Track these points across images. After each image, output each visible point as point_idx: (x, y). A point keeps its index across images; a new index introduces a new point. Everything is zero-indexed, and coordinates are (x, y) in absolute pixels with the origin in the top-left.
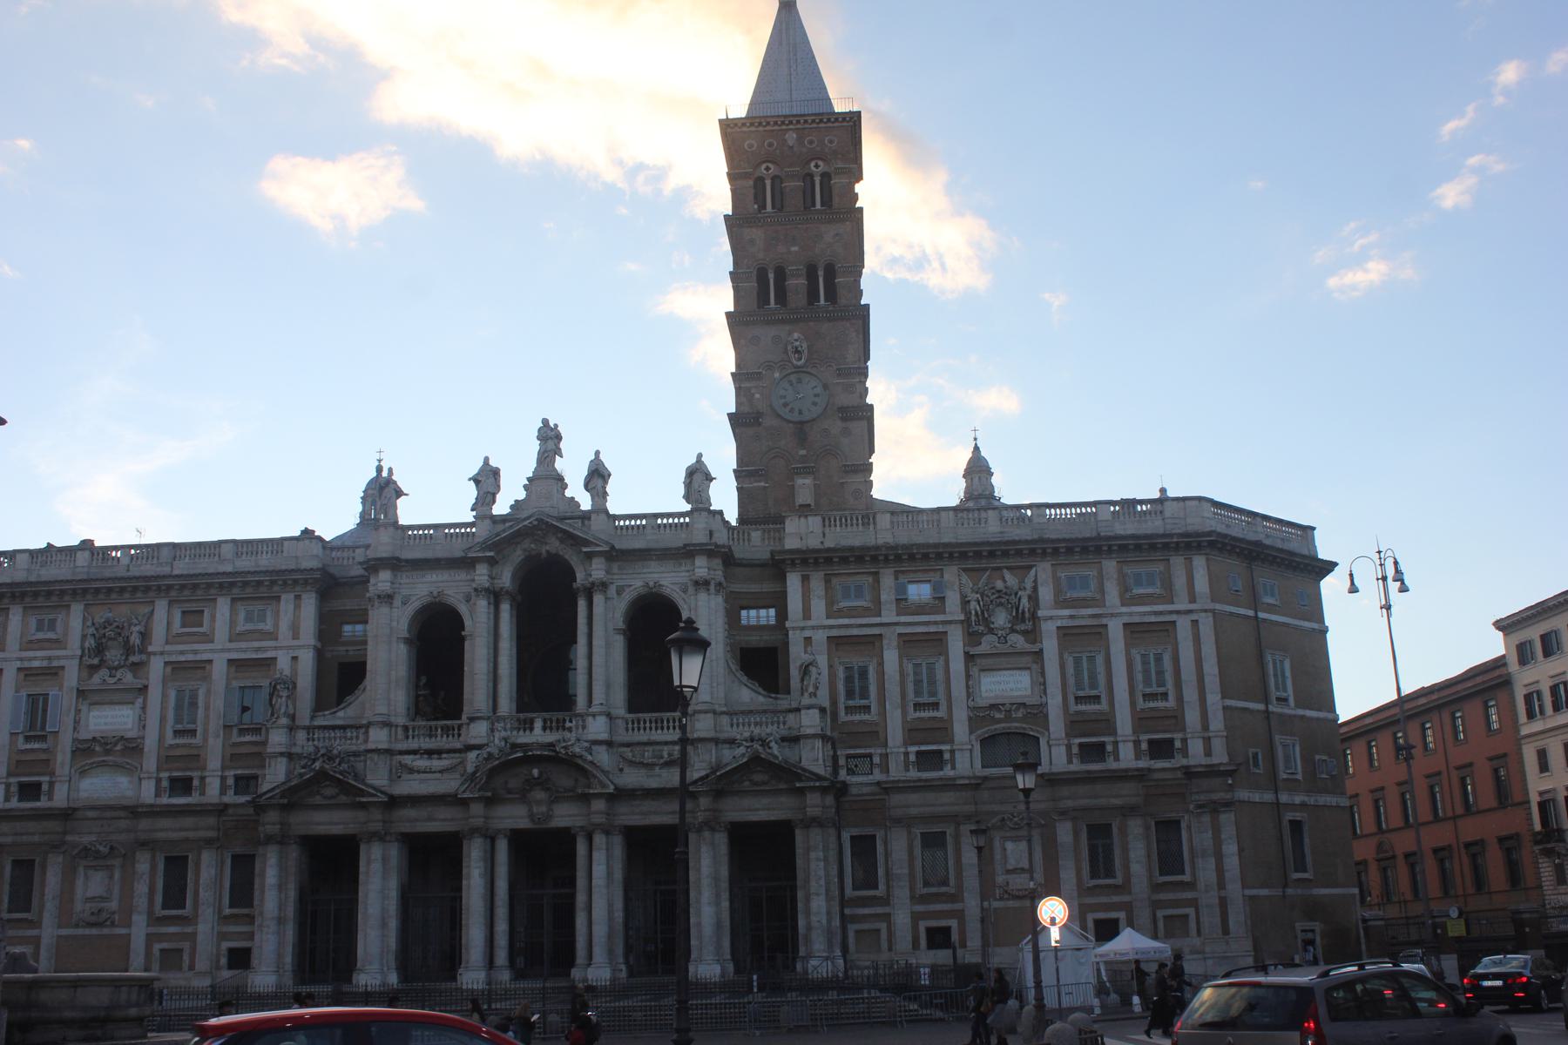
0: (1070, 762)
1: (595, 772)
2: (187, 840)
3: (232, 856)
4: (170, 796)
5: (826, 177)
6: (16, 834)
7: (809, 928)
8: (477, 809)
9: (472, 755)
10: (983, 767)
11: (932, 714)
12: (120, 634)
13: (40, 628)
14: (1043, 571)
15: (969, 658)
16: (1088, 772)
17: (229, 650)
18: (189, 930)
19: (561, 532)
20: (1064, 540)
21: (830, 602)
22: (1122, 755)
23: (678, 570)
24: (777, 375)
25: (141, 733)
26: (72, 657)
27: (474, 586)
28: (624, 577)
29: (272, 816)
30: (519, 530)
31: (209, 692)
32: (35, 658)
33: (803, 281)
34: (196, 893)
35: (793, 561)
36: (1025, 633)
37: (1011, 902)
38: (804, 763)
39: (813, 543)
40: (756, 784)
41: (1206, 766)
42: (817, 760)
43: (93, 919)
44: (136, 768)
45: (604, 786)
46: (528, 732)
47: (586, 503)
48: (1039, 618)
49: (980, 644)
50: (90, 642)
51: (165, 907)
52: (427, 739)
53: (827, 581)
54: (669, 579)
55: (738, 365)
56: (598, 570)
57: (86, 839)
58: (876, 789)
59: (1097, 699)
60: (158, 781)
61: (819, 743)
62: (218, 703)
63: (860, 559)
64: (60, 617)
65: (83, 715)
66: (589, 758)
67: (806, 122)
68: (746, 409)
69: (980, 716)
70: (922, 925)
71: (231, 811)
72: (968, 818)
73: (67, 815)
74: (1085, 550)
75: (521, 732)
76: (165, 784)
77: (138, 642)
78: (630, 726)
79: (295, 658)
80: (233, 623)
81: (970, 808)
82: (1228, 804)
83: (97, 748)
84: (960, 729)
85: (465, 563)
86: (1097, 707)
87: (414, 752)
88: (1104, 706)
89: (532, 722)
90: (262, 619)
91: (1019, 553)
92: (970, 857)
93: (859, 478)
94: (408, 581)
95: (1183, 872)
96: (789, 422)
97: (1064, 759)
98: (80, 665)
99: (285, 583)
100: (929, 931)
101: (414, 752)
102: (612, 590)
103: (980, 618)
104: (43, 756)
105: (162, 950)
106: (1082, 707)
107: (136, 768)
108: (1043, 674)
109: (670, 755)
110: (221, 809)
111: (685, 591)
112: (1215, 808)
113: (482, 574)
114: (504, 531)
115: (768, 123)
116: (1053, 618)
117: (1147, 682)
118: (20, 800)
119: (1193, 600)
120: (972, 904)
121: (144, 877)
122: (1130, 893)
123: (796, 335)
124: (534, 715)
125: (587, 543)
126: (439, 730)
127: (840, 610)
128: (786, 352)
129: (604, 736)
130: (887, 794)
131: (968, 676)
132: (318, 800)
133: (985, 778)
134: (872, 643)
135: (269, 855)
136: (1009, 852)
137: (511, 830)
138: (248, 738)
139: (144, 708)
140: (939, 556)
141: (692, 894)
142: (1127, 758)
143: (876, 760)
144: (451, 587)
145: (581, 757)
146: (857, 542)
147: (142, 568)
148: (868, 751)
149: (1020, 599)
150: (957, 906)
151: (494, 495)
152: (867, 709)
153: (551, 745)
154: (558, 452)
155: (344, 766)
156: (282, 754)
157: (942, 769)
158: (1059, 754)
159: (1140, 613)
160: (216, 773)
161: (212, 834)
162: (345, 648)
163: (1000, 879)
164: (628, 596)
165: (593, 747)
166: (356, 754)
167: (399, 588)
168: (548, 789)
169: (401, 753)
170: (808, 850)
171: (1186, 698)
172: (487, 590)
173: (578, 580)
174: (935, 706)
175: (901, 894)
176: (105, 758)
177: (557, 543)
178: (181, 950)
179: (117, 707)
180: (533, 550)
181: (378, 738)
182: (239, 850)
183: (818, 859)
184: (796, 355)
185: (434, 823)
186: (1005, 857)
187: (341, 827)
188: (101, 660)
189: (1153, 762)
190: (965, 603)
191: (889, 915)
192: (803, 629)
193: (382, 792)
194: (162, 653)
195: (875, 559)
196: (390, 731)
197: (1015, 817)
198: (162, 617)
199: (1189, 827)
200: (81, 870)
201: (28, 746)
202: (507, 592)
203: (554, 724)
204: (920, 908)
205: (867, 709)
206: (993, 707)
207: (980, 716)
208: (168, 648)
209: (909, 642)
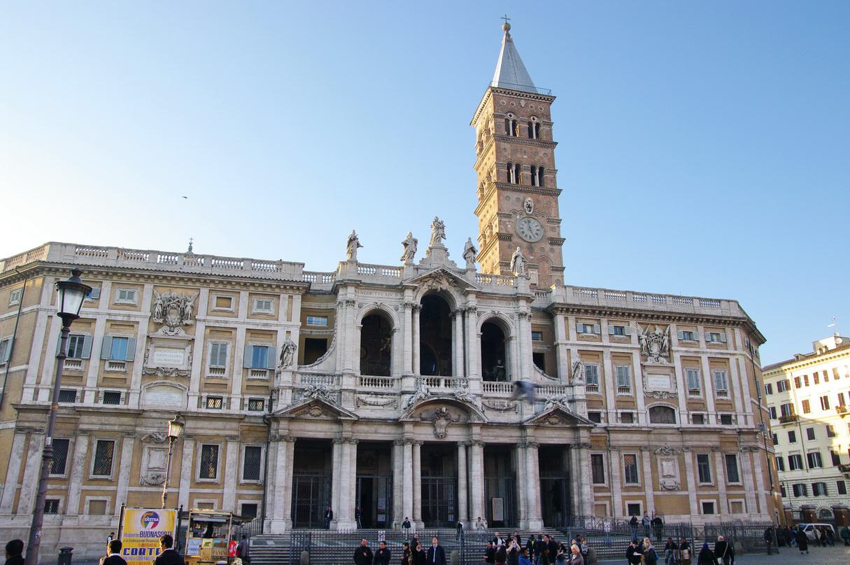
0: (689, 423)
1: (477, 411)
2: (218, 436)
3: (246, 447)
4: (207, 408)
5: (538, 125)
6: (101, 424)
7: (581, 503)
8: (408, 428)
9: (407, 397)
10: (651, 422)
11: (628, 394)
12: (179, 306)
13: (121, 297)
14: (673, 327)
15: (643, 367)
16: (699, 428)
17: (248, 323)
18: (219, 491)
20: (684, 314)
24: (518, 217)
25: (189, 368)
26: (145, 317)
29: (283, 424)
30: (430, 275)
31: (234, 347)
32: (119, 315)
33: (529, 173)
34: (224, 468)
35: (562, 308)
36: (665, 357)
38: (578, 413)
39: (570, 301)
40: (552, 424)
41: (748, 429)
42: (585, 413)
43: (153, 482)
44: (186, 389)
45: (480, 418)
46: (437, 386)
47: (462, 264)
48: (672, 351)
49: (646, 360)
50: (158, 309)
51: (201, 477)
52: (373, 386)
53: (577, 322)
54: (504, 311)
55: (499, 210)
56: (472, 301)
57: (151, 431)
58: (603, 431)
60: (200, 398)
61: (585, 404)
62: (240, 354)
63: (594, 312)
64: (137, 291)
65: (150, 353)
66: (475, 403)
67: (530, 97)
68: (504, 232)
69: (649, 396)
70: (627, 502)
71: (247, 420)
72: (646, 447)
73: (138, 414)
74: (692, 320)
75: (433, 386)
76: (204, 400)
77: (190, 312)
78: (486, 388)
79: (288, 332)
80: (250, 308)
81: (646, 443)
82: (757, 448)
83: (159, 374)
84: (640, 402)
85: (400, 289)
86: (697, 397)
87: (368, 393)
88: (701, 396)
89: (439, 381)
90: (268, 306)
91: (664, 318)
92: (647, 468)
93: (558, 274)
95: (738, 481)
96: (525, 241)
97: (687, 422)
98: (149, 322)
99: (285, 287)
100: (629, 505)
101: (368, 393)
104: (123, 376)
105: (199, 503)
107: (186, 389)
109: (508, 405)
110: (241, 419)
111: (512, 318)
112: (752, 450)
113: (409, 296)
114: (424, 273)
115: (512, 94)
116: (678, 351)
117: (719, 386)
118: (104, 403)
119: (736, 349)
120: (649, 493)
121: (190, 457)
122: (718, 490)
123: (529, 199)
124: (441, 377)
125: (467, 285)
126: (380, 383)
127: (583, 337)
129: (479, 392)
130: (609, 434)
131: (643, 376)
132: (308, 416)
133: (654, 428)
134: (598, 354)
135: (280, 448)
136: (664, 466)
137: (425, 441)
138: (256, 377)
139: (191, 353)
140: (629, 315)
141: (521, 482)
142: (713, 423)
143: (602, 415)
144: (388, 302)
145: (471, 402)
146: (589, 303)
147: (193, 268)
150: (643, 493)
151: (414, 253)
152: (596, 389)
154: (443, 236)
155: (330, 398)
156: (290, 388)
157: (632, 422)
158: (684, 418)
159: (714, 352)
160: (238, 396)
161: (234, 433)
162: (309, 330)
163: (661, 480)
164: (483, 318)
166: (334, 392)
168: (447, 420)
169: (360, 393)
170: (580, 460)
171: (736, 395)
174: (627, 390)
175: (617, 486)
176: (165, 381)
178: (213, 504)
179: (173, 350)
181: (348, 383)
182: (251, 444)
183: (587, 466)
185: (379, 435)
187: (323, 434)
188: (163, 321)
190: (640, 339)
191: (611, 497)
192: (566, 344)
193: (354, 415)
194: (204, 320)
195: (600, 313)
198: (205, 299)
199: (740, 458)
200: (146, 450)
201: (111, 369)
205: (596, 389)
207: (649, 396)
208: (208, 318)
209: (615, 356)
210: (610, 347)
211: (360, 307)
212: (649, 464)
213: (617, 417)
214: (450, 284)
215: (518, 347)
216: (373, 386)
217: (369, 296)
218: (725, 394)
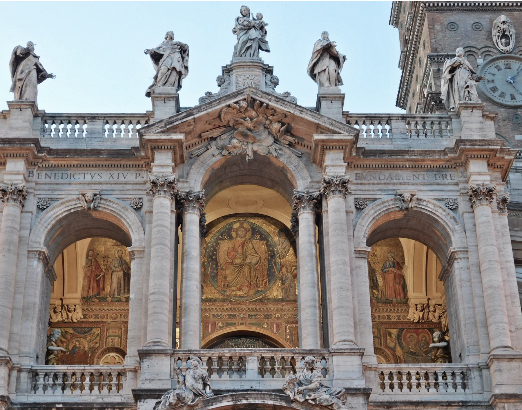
19: (279, 122)
23: (443, 182)
27: (153, 178)
28: (366, 187)
94: (48, 180)
102: (351, 199)
111: (454, 209)
124: (246, 351)
128: (489, 37)
129: (360, 384)
153: (280, 393)
165: (350, 399)
167: (35, 190)
172: (170, 184)
173: (300, 189)
177: (271, 140)
180: (235, 147)
184: (503, 40)
196: (9, 376)
202: (198, 198)
203: (276, 366)
211: (41, 209)
214: (276, 141)
215: (474, 274)
216: (68, 391)
217: (67, 181)
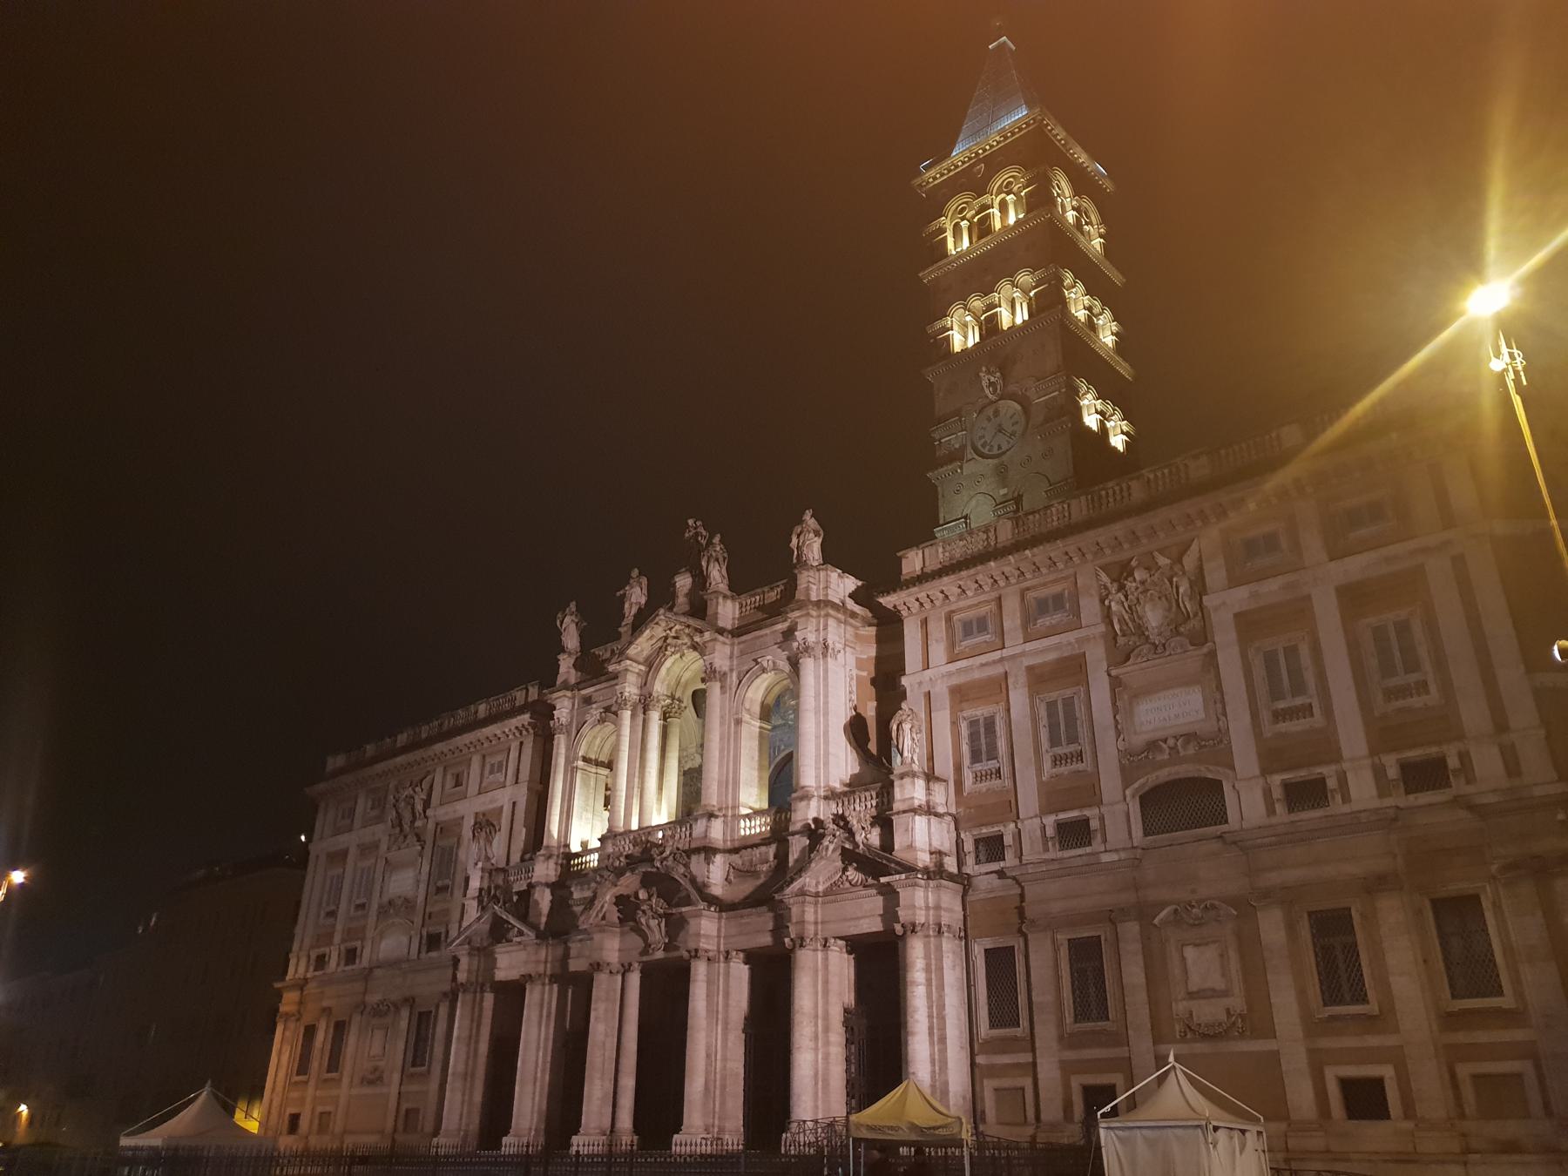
0: (1271, 811)
10: (1146, 834)
15: (1116, 683)
21: (952, 645)
22: (1354, 792)
37: (1198, 1045)
59: (1307, 710)
70: (1076, 1083)
84: (1110, 783)
92: (1135, 973)
95: (1500, 993)
103: (1130, 624)
106: (1283, 727)
108: (1219, 687)
136: (1189, 962)
143: (1008, 840)
148: (996, 829)
149: (1177, 588)
163: (1180, 1007)
175: (1046, 1034)
186: (1185, 971)
189: (1411, 797)
197: (1193, 906)
199: (1497, 906)
204: (1070, 1055)
206: (1153, 746)
210: (1023, 654)
212: (1140, 959)
213: (1045, 843)
218: (1423, 687)
